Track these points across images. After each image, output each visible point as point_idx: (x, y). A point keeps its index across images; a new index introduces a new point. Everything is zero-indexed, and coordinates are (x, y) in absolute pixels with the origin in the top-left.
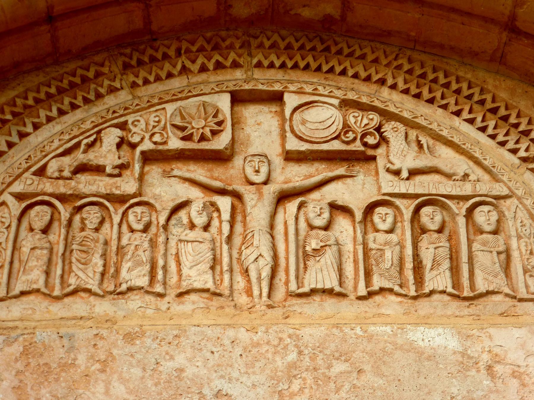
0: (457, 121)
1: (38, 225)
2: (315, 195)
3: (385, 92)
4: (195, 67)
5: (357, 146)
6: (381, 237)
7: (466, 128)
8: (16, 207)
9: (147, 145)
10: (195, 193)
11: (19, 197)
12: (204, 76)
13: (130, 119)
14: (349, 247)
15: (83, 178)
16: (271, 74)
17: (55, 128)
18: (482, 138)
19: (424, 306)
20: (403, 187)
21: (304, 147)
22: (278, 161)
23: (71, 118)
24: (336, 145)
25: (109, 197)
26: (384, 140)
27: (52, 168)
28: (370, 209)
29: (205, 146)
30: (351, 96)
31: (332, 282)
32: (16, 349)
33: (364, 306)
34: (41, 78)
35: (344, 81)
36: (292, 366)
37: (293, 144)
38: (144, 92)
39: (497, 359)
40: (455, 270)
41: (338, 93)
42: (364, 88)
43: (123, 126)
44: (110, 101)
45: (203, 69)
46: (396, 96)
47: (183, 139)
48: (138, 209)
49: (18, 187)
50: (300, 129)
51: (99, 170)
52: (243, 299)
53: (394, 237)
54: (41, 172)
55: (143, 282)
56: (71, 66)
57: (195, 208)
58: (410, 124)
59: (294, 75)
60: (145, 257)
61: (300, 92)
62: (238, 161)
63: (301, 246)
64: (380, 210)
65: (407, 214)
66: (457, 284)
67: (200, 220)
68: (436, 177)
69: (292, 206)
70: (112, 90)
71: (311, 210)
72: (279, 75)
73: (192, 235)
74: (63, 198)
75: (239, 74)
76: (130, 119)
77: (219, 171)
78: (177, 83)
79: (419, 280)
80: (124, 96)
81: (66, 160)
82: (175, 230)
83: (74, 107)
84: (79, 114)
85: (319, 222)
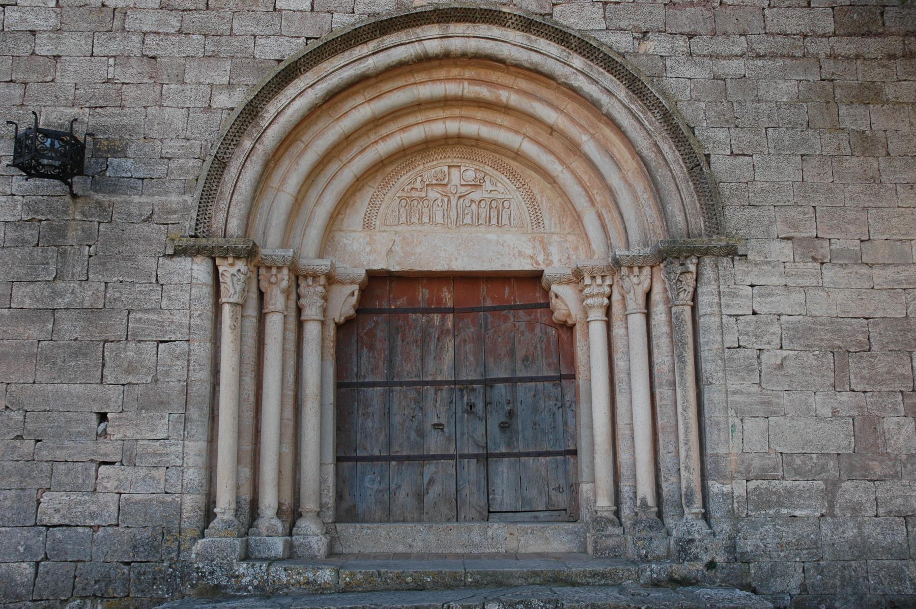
0: (503, 176)
1: (404, 205)
2: (467, 197)
3: (486, 167)
4: (439, 158)
5: (478, 183)
6: (482, 210)
7: (504, 178)
8: (398, 200)
9: (428, 182)
10: (439, 196)
11: (399, 197)
12: (441, 161)
13: (423, 174)
14: (474, 212)
15: (413, 192)
16: (458, 160)
17: (404, 177)
18: (508, 181)
19: (490, 229)
20: (488, 196)
21: (465, 183)
22: (459, 186)
23: (409, 174)
24: (473, 183)
25: (419, 197)
26: (485, 181)
27: (405, 190)
28: (480, 201)
29: (441, 183)
30: (478, 168)
31: (470, 222)
32: (401, 238)
33: (477, 228)
34: (402, 161)
35: (476, 163)
36: (460, 243)
37: (463, 183)
38: (426, 166)
39: (505, 242)
40: (498, 218)
41: (475, 167)
42: (482, 165)
43: (421, 176)
44: (418, 168)
45: (441, 158)
46: (489, 168)
47: (437, 180)
48: (426, 201)
49: (398, 195)
50: (464, 178)
51: (416, 189)
52: (450, 225)
53: (485, 210)
54: (403, 190)
55: (428, 221)
56: (408, 157)
57: (439, 200)
58: (491, 176)
59: (464, 160)
60: (428, 215)
61: (465, 166)
62: (449, 186)
63: (463, 212)
64: (482, 202)
65: (488, 203)
66: (498, 223)
67: (440, 204)
68: (496, 192)
69: (462, 200)
70: (419, 165)
71: (466, 201)
72: (460, 160)
73: (438, 208)
74: (408, 197)
75: (450, 160)
76: (423, 174)
77: (444, 189)
78: (435, 163)
79: (490, 221)
80: (422, 167)
81: (409, 186)
82: (435, 206)
83: (410, 170)
84: (411, 173)
85: (468, 205)
